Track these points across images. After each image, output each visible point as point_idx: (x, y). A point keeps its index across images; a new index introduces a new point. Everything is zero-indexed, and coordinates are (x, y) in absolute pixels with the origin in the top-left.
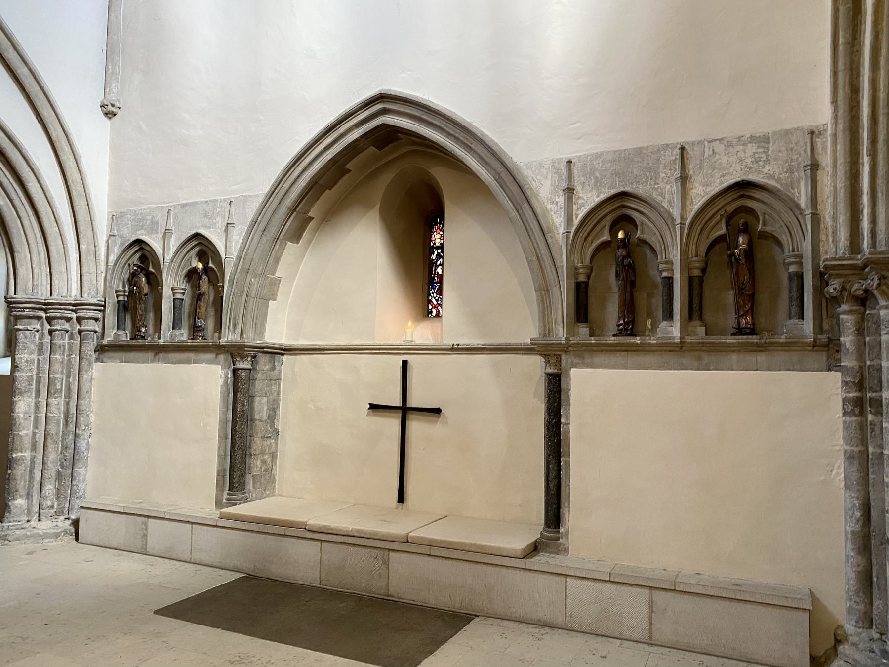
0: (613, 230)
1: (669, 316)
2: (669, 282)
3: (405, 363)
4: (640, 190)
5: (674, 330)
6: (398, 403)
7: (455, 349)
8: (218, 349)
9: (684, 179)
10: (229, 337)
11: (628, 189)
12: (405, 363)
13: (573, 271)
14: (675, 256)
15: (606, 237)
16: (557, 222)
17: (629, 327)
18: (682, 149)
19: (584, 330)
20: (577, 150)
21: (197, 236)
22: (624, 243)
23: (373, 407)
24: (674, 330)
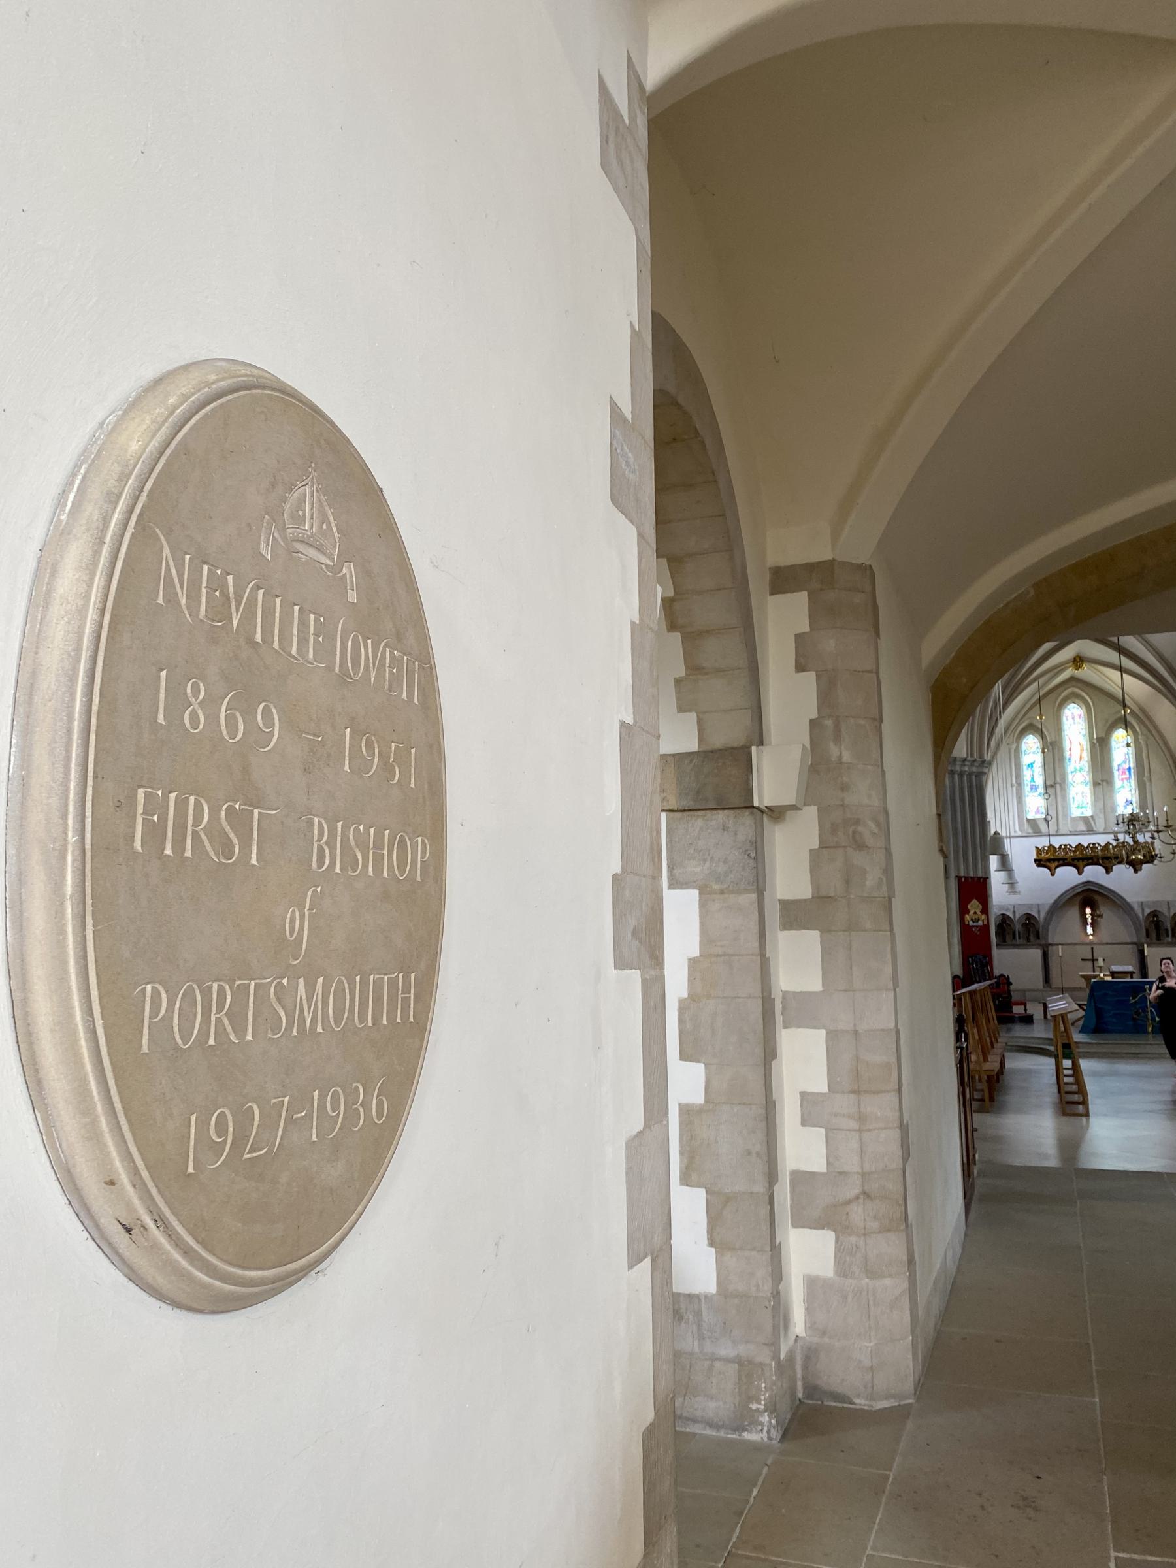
0: (1154, 917)
1: (1168, 936)
2: (1167, 930)
3: (1092, 948)
4: (1158, 909)
5: (1170, 939)
6: (1090, 957)
7: (1107, 944)
8: (1040, 945)
9: (1169, 908)
10: (1043, 942)
11: (1156, 909)
12: (1092, 948)
13: (1145, 926)
14: (1169, 926)
15: (1152, 919)
16: (1140, 915)
17: (1158, 938)
18: (1168, 903)
19: (1148, 940)
20: (1143, 899)
21: (1028, 914)
22: (1156, 921)
23: (1083, 960)
24: (1170, 939)
